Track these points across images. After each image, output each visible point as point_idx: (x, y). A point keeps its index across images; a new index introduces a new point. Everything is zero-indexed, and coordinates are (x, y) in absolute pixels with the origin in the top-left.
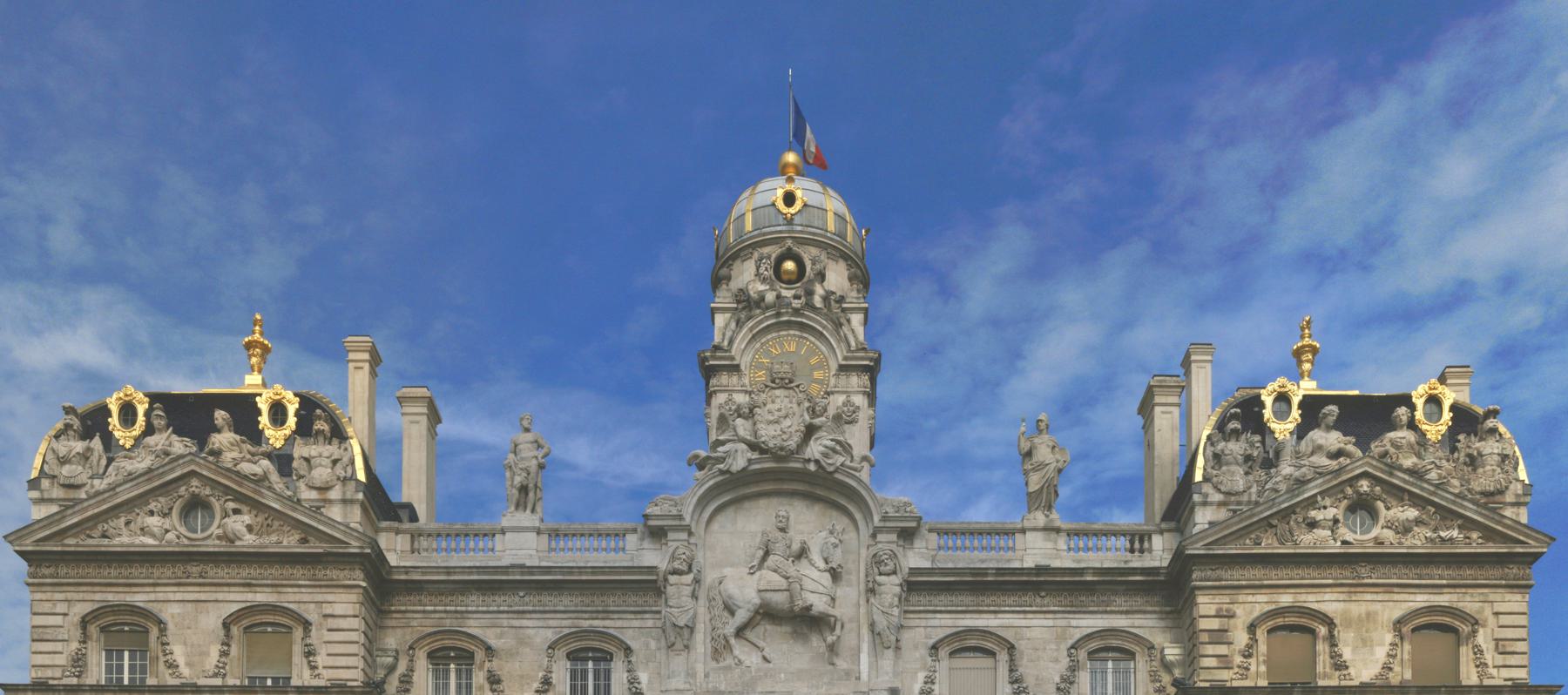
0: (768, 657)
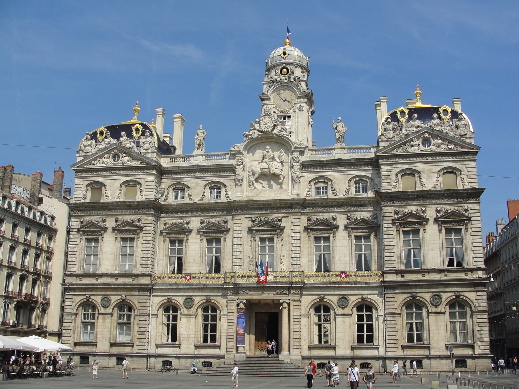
0: (264, 186)
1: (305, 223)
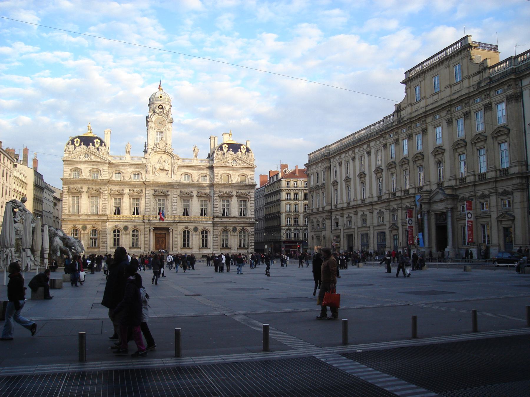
1: (179, 193)
